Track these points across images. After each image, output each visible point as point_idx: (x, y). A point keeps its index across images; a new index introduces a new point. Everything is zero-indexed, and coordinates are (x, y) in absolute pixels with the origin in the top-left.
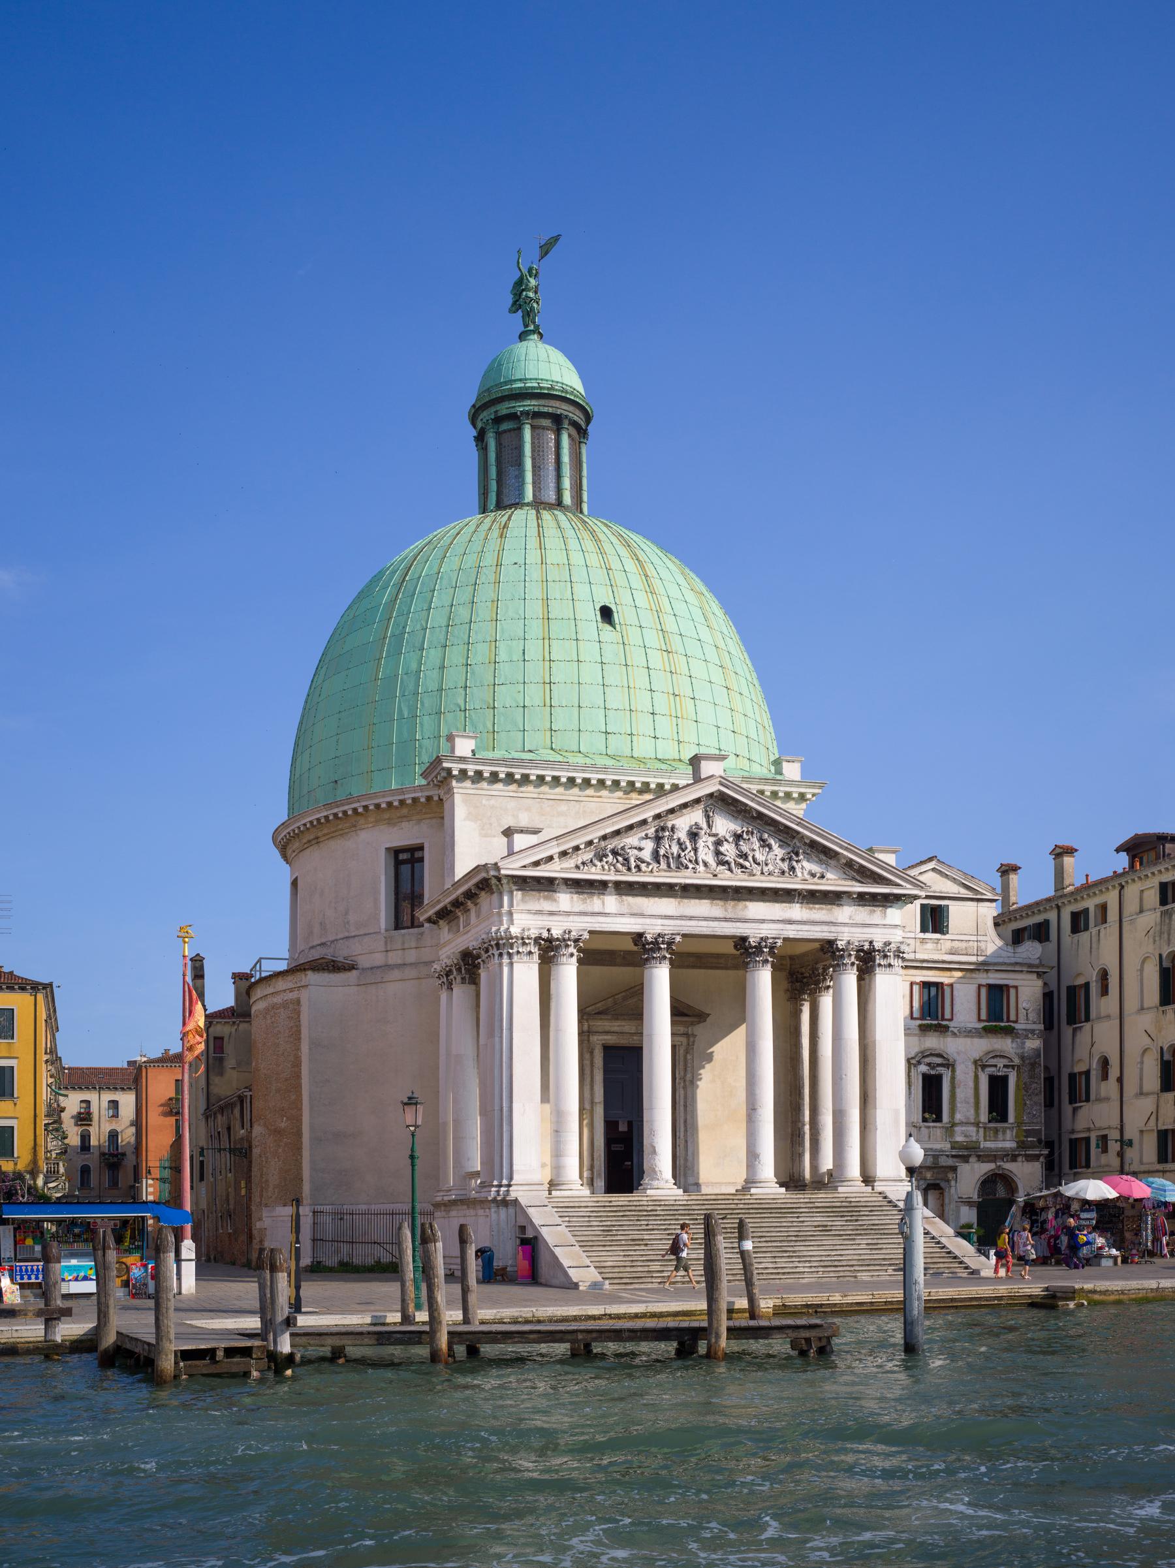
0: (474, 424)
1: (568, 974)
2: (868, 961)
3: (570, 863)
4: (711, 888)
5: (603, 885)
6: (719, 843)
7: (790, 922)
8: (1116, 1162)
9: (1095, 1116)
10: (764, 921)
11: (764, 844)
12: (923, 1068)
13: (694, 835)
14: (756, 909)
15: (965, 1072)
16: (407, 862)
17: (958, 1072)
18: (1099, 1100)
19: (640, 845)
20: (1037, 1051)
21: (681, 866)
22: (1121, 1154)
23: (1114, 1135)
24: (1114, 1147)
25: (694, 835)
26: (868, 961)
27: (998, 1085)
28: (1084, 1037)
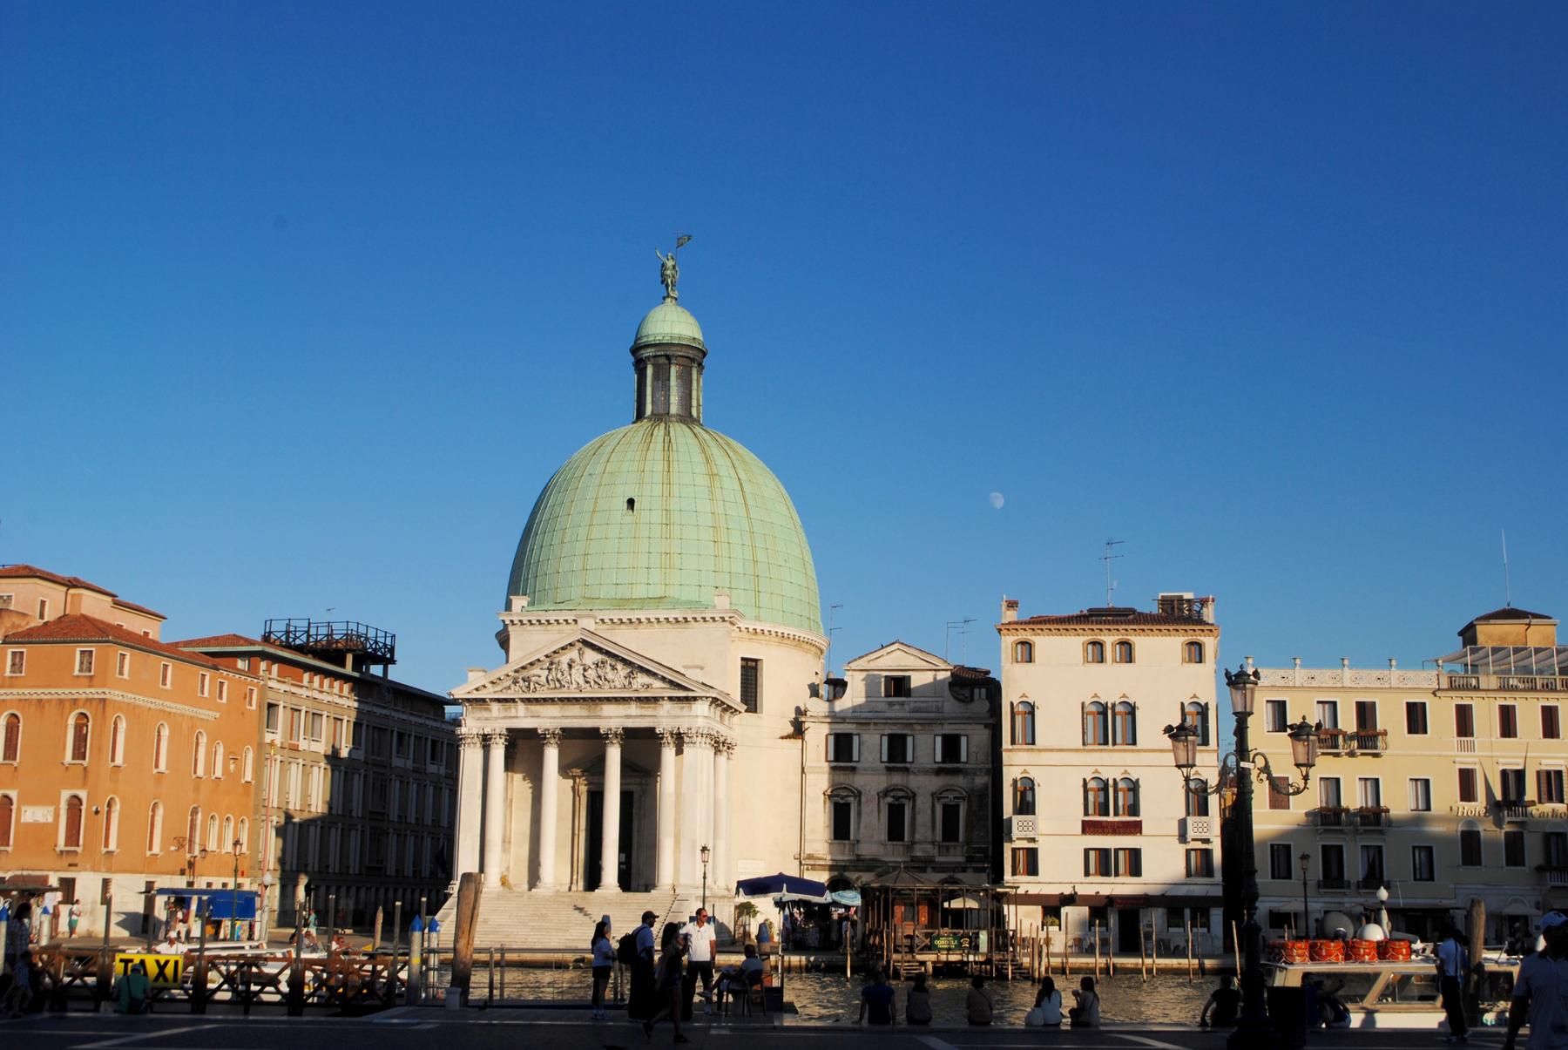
2: (679, 740)
3: (498, 688)
4: (577, 700)
5: (513, 700)
7: (628, 717)
10: (613, 719)
11: (614, 668)
12: (889, 800)
13: (570, 666)
14: (608, 709)
15: (923, 803)
17: (918, 802)
19: (539, 673)
20: (986, 787)
25: (570, 666)
26: (679, 740)
27: (950, 813)
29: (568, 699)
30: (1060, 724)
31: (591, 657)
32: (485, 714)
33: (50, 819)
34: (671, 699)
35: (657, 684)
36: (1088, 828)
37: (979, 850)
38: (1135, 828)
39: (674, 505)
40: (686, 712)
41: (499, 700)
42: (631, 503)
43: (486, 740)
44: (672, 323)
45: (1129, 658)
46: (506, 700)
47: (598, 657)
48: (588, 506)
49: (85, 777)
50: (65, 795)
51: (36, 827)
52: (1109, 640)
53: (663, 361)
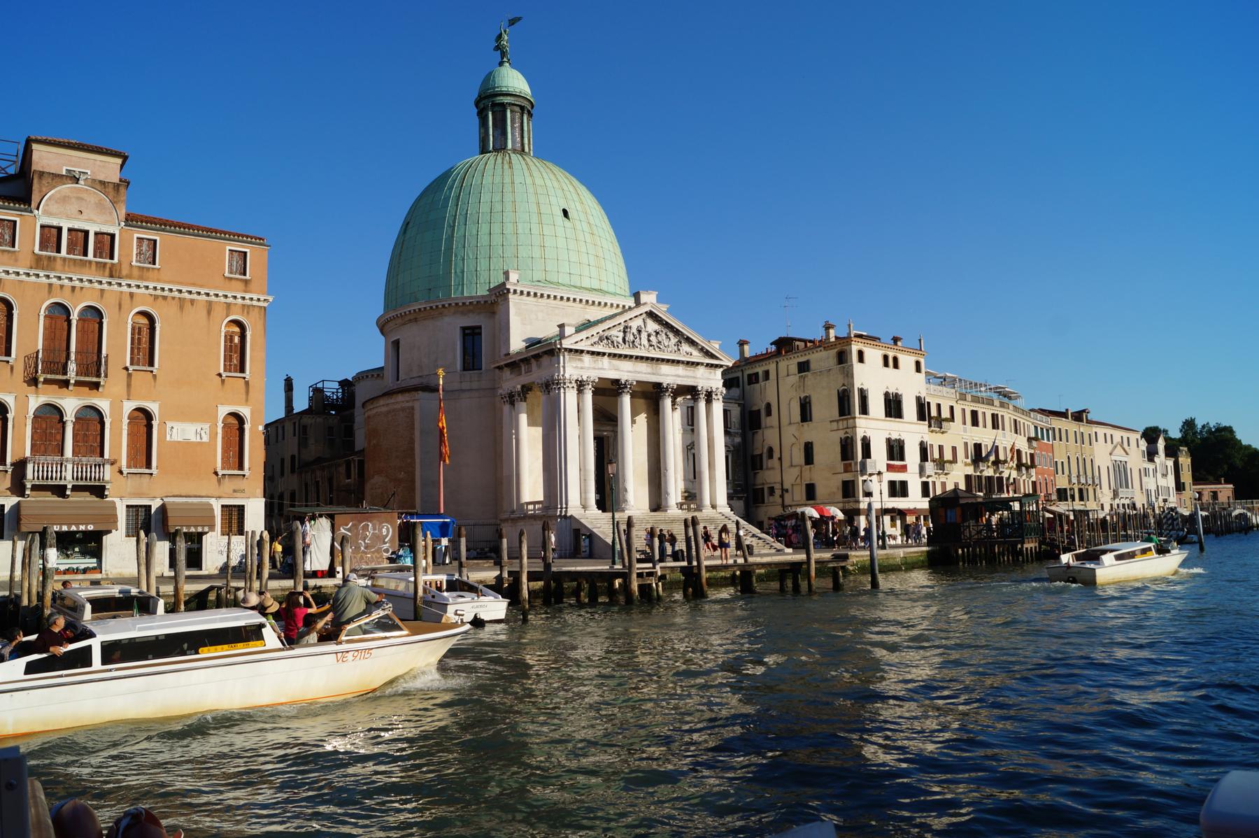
0: (477, 106)
1: (588, 396)
3: (589, 342)
4: (647, 358)
5: (604, 354)
6: (649, 335)
8: (780, 500)
9: (769, 476)
10: (670, 376)
13: (639, 331)
14: (665, 369)
16: (471, 336)
18: (768, 469)
21: (634, 347)
22: (782, 496)
23: (777, 486)
24: (778, 492)
25: (639, 331)
28: (759, 437)
29: (642, 358)
30: (877, 405)
31: (652, 326)
32: (579, 364)
33: (205, 439)
34: (707, 365)
35: (695, 353)
36: (890, 468)
37: (738, 485)
38: (903, 469)
39: (592, 222)
40: (712, 376)
41: (593, 353)
42: (565, 213)
43: (581, 386)
44: (514, 81)
45: (896, 366)
46: (598, 354)
47: (656, 327)
48: (534, 208)
49: (247, 392)
50: (223, 411)
51: (187, 444)
52: (891, 354)
53: (517, 109)
